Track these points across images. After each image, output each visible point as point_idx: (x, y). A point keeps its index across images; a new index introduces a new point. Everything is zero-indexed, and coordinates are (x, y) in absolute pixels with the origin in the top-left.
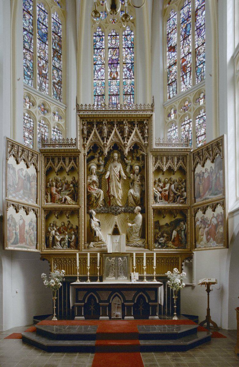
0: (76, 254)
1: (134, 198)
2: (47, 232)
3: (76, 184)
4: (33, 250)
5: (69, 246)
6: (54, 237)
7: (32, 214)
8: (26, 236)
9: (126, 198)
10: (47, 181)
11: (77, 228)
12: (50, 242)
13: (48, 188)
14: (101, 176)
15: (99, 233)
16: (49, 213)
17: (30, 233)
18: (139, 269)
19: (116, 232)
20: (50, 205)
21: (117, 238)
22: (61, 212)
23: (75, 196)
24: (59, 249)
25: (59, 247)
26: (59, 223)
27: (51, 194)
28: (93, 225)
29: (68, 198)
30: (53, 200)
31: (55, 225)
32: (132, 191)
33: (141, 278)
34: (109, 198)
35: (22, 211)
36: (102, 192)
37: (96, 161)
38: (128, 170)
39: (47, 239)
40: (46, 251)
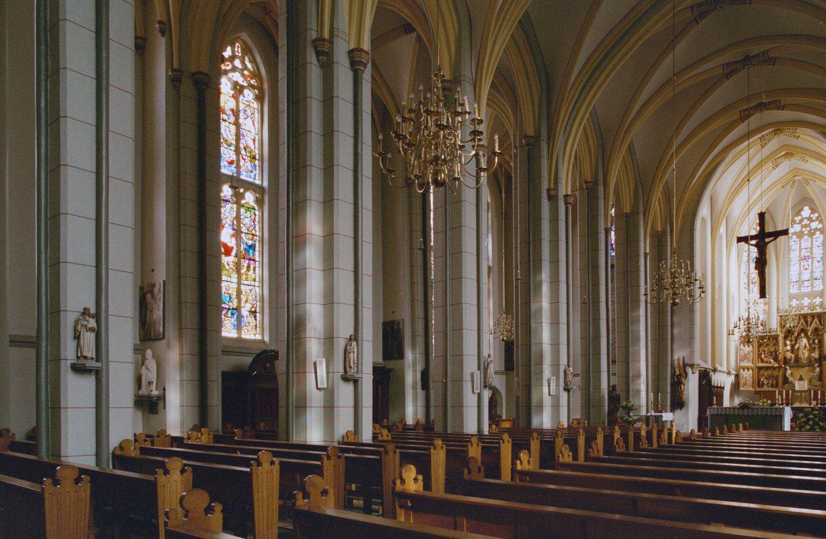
0: (775, 391)
1: (815, 359)
2: (759, 380)
3: (776, 351)
4: (751, 389)
5: (772, 386)
6: (763, 382)
7: (751, 371)
8: (748, 382)
9: (809, 358)
10: (759, 351)
11: (777, 376)
12: (760, 384)
13: (759, 355)
14: (793, 346)
15: (791, 379)
16: (760, 369)
17: (750, 381)
18: (816, 398)
19: (801, 379)
20: (760, 365)
21: (801, 382)
22: (767, 368)
23: (776, 359)
24: (766, 388)
25: (766, 387)
26: (766, 374)
27: (761, 359)
28: (787, 375)
29: (772, 361)
30: (762, 361)
31: (763, 375)
32: (813, 355)
33: (817, 404)
34: (797, 359)
35: (746, 370)
36: (793, 356)
37: (790, 338)
38: (811, 342)
39: (759, 383)
40: (758, 389)
